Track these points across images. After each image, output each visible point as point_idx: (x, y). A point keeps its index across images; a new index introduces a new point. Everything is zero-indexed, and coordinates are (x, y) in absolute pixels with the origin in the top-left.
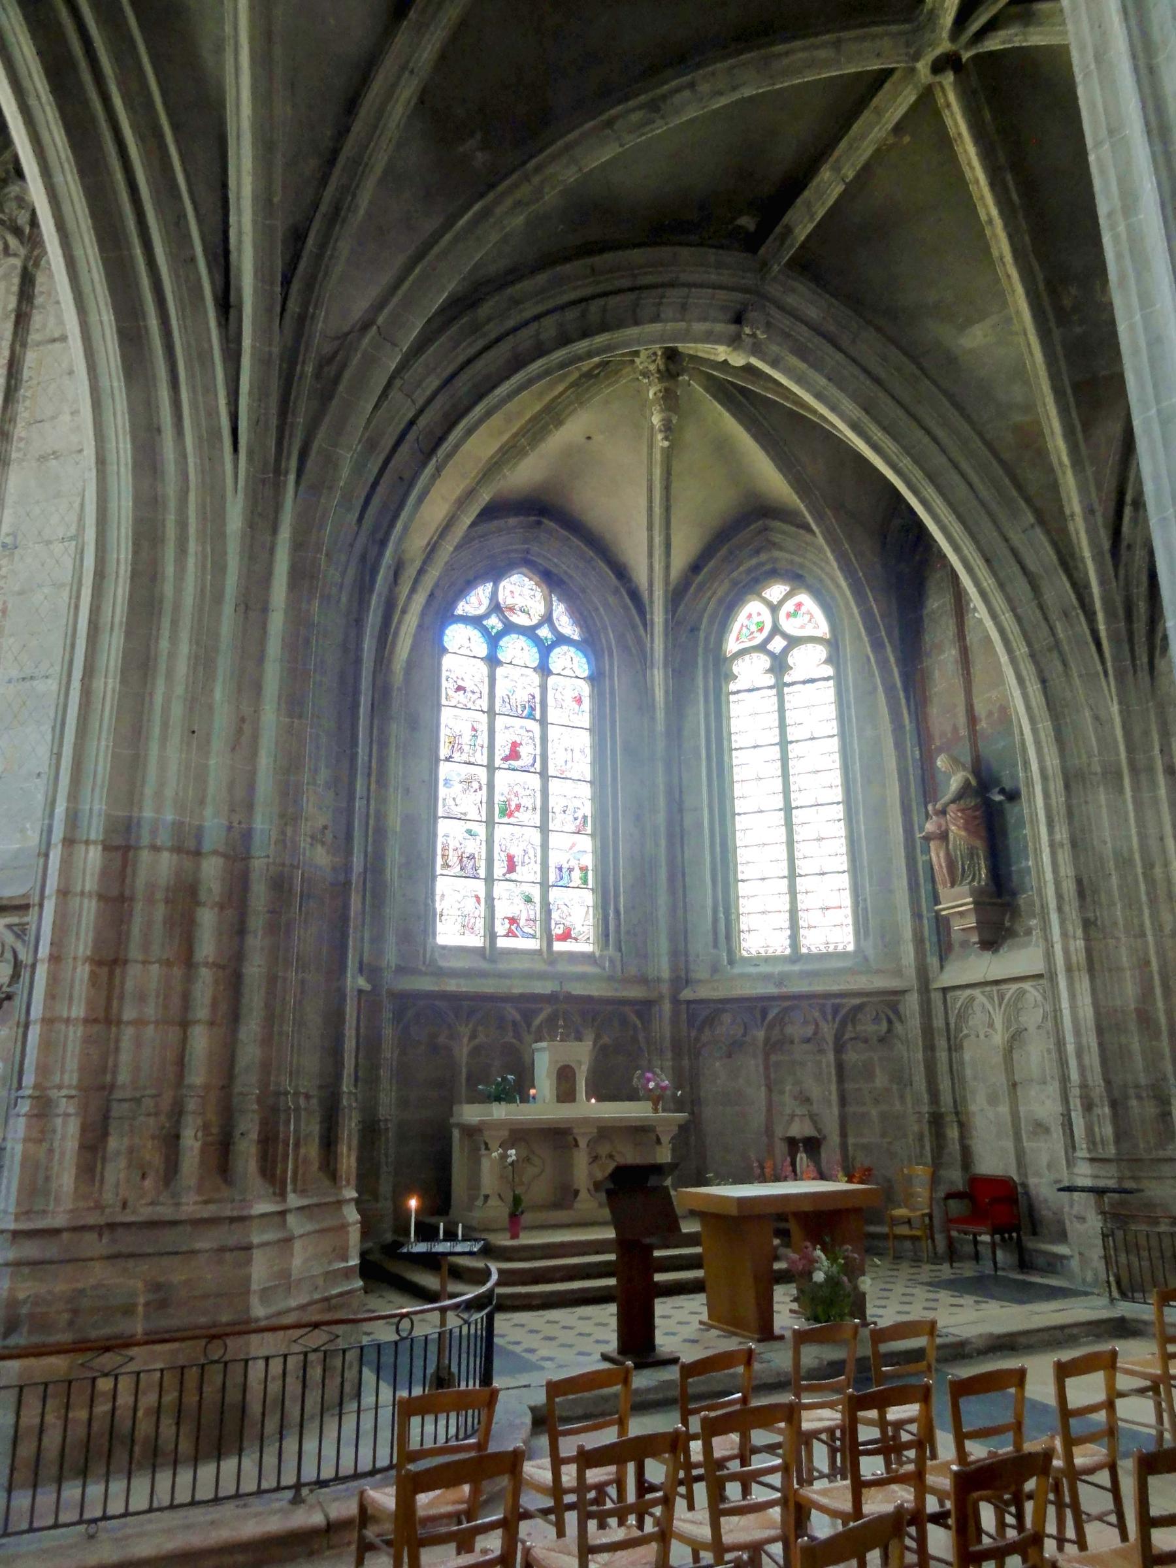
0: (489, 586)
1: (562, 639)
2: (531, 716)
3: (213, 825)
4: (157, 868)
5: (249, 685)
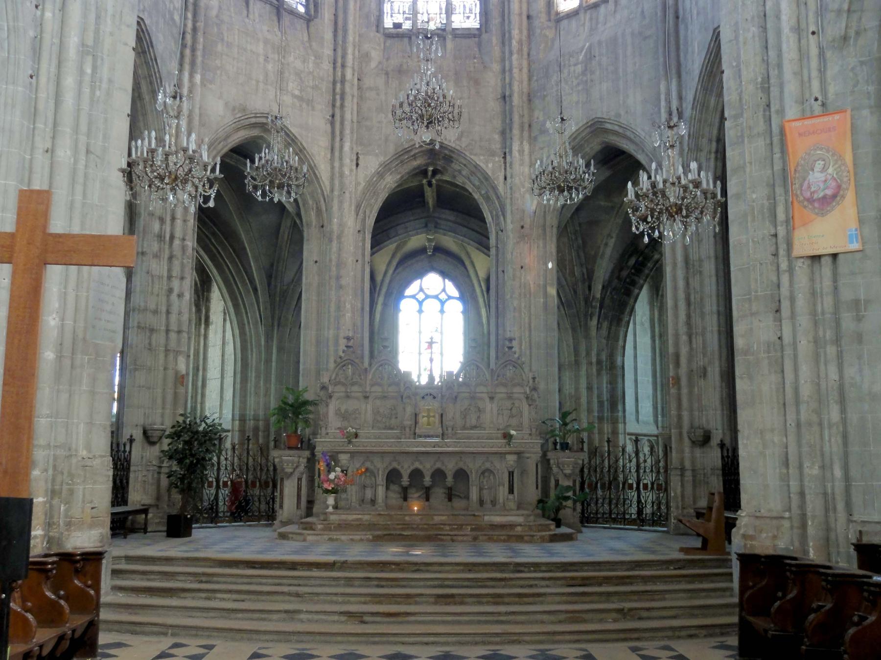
0: (419, 281)
1: (450, 298)
3: (261, 413)
4: (251, 424)
5: (267, 380)
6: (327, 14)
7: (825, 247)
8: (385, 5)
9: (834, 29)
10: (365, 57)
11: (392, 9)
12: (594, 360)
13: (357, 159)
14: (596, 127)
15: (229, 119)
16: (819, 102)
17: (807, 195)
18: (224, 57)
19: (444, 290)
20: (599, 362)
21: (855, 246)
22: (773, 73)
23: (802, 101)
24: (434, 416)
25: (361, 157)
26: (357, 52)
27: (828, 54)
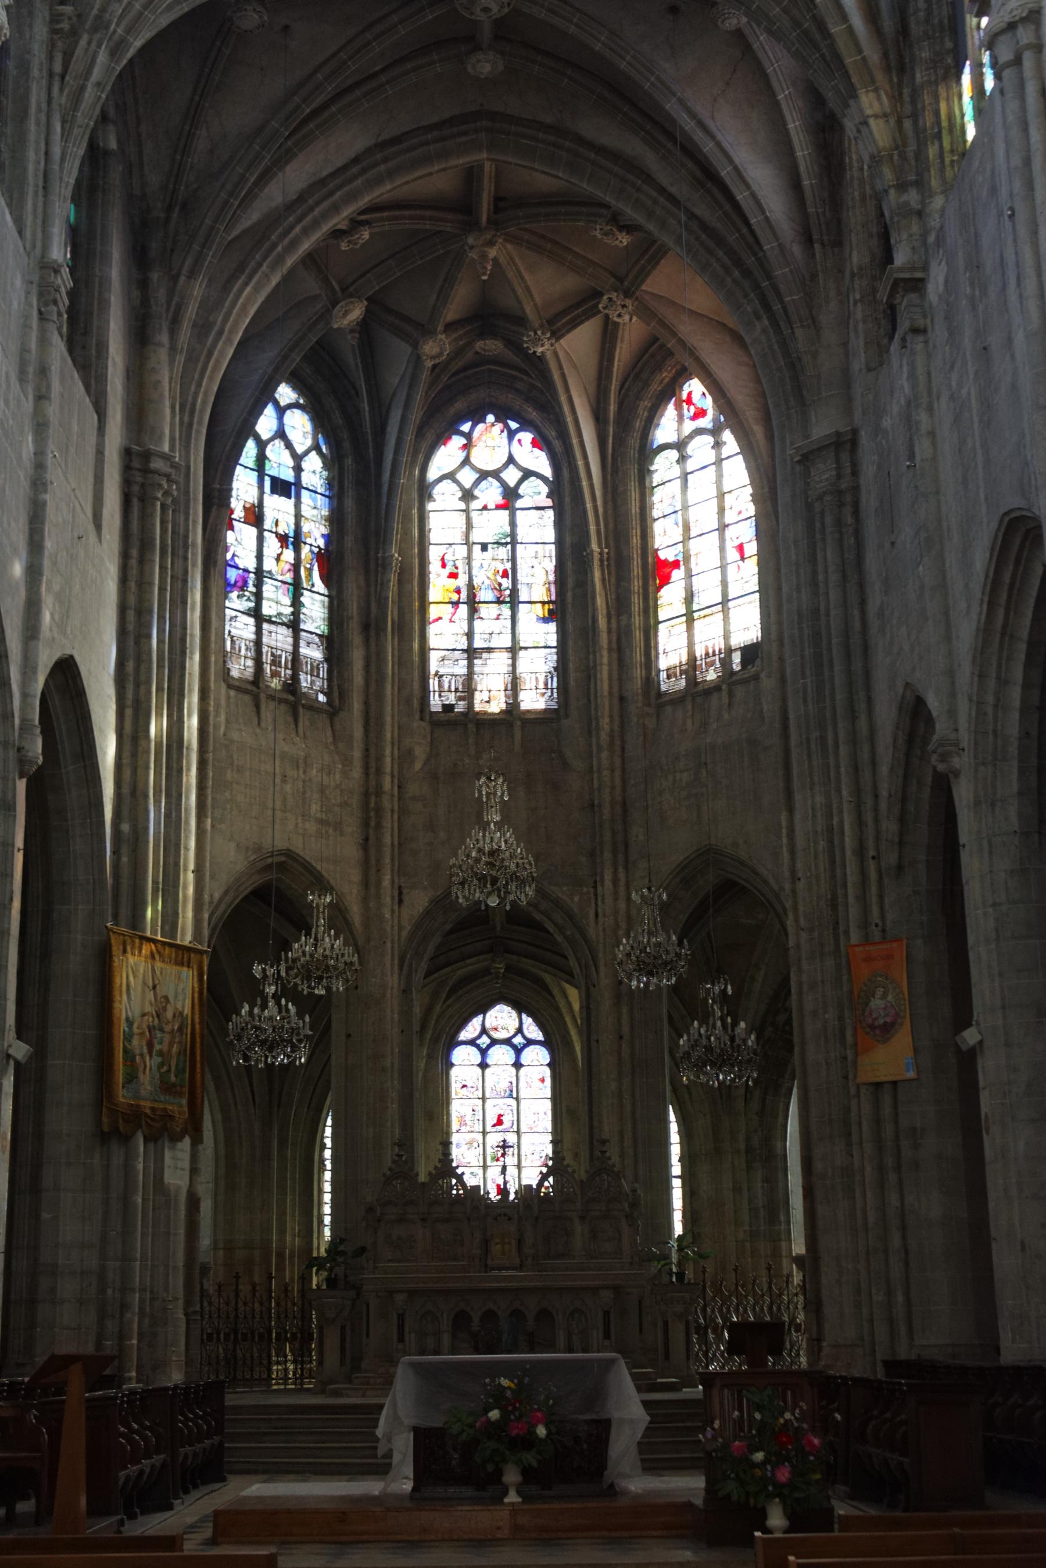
1: (530, 1042)
2: (511, 1096)
6: (357, 706)
7: (884, 1075)
8: (431, 681)
9: (891, 858)
10: (405, 756)
11: (440, 685)
12: (742, 1146)
13: (400, 893)
14: (708, 856)
15: (241, 866)
16: (880, 928)
17: (870, 1021)
18: (235, 785)
19: (520, 1030)
20: (749, 1150)
21: (911, 1074)
22: (840, 892)
23: (865, 924)
24: (509, 1243)
25: (405, 891)
26: (396, 752)
27: (886, 881)
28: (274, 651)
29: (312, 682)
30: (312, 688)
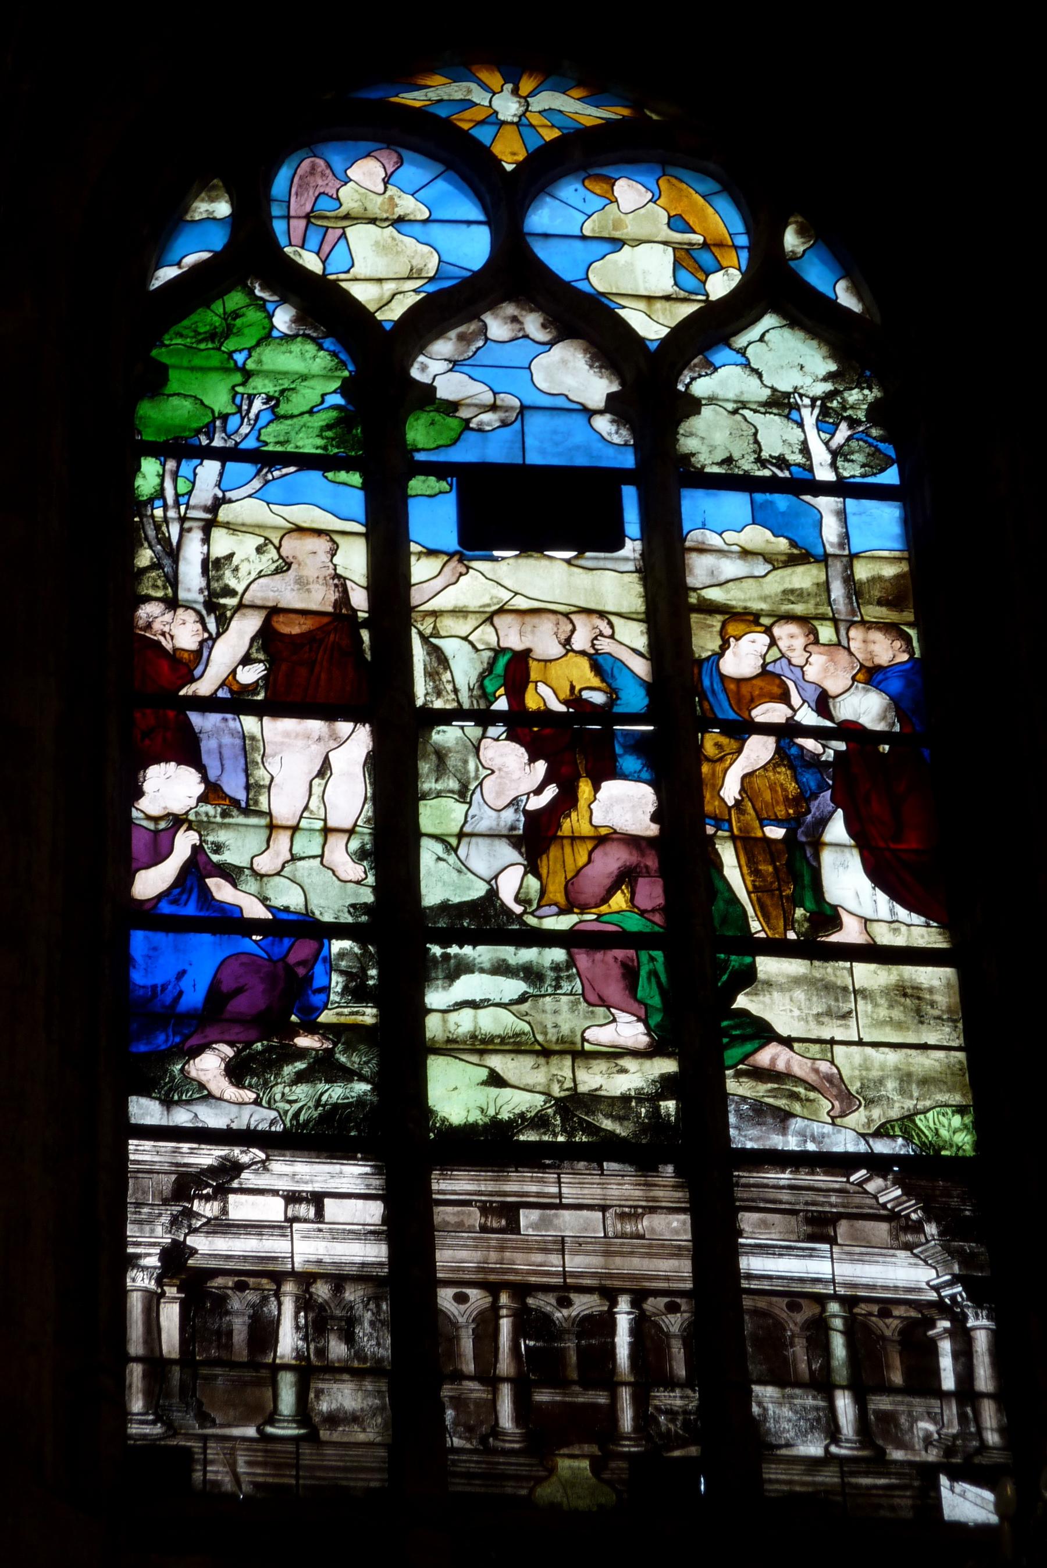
28: (543, 1302)
29: (874, 1430)
30: (878, 1462)
